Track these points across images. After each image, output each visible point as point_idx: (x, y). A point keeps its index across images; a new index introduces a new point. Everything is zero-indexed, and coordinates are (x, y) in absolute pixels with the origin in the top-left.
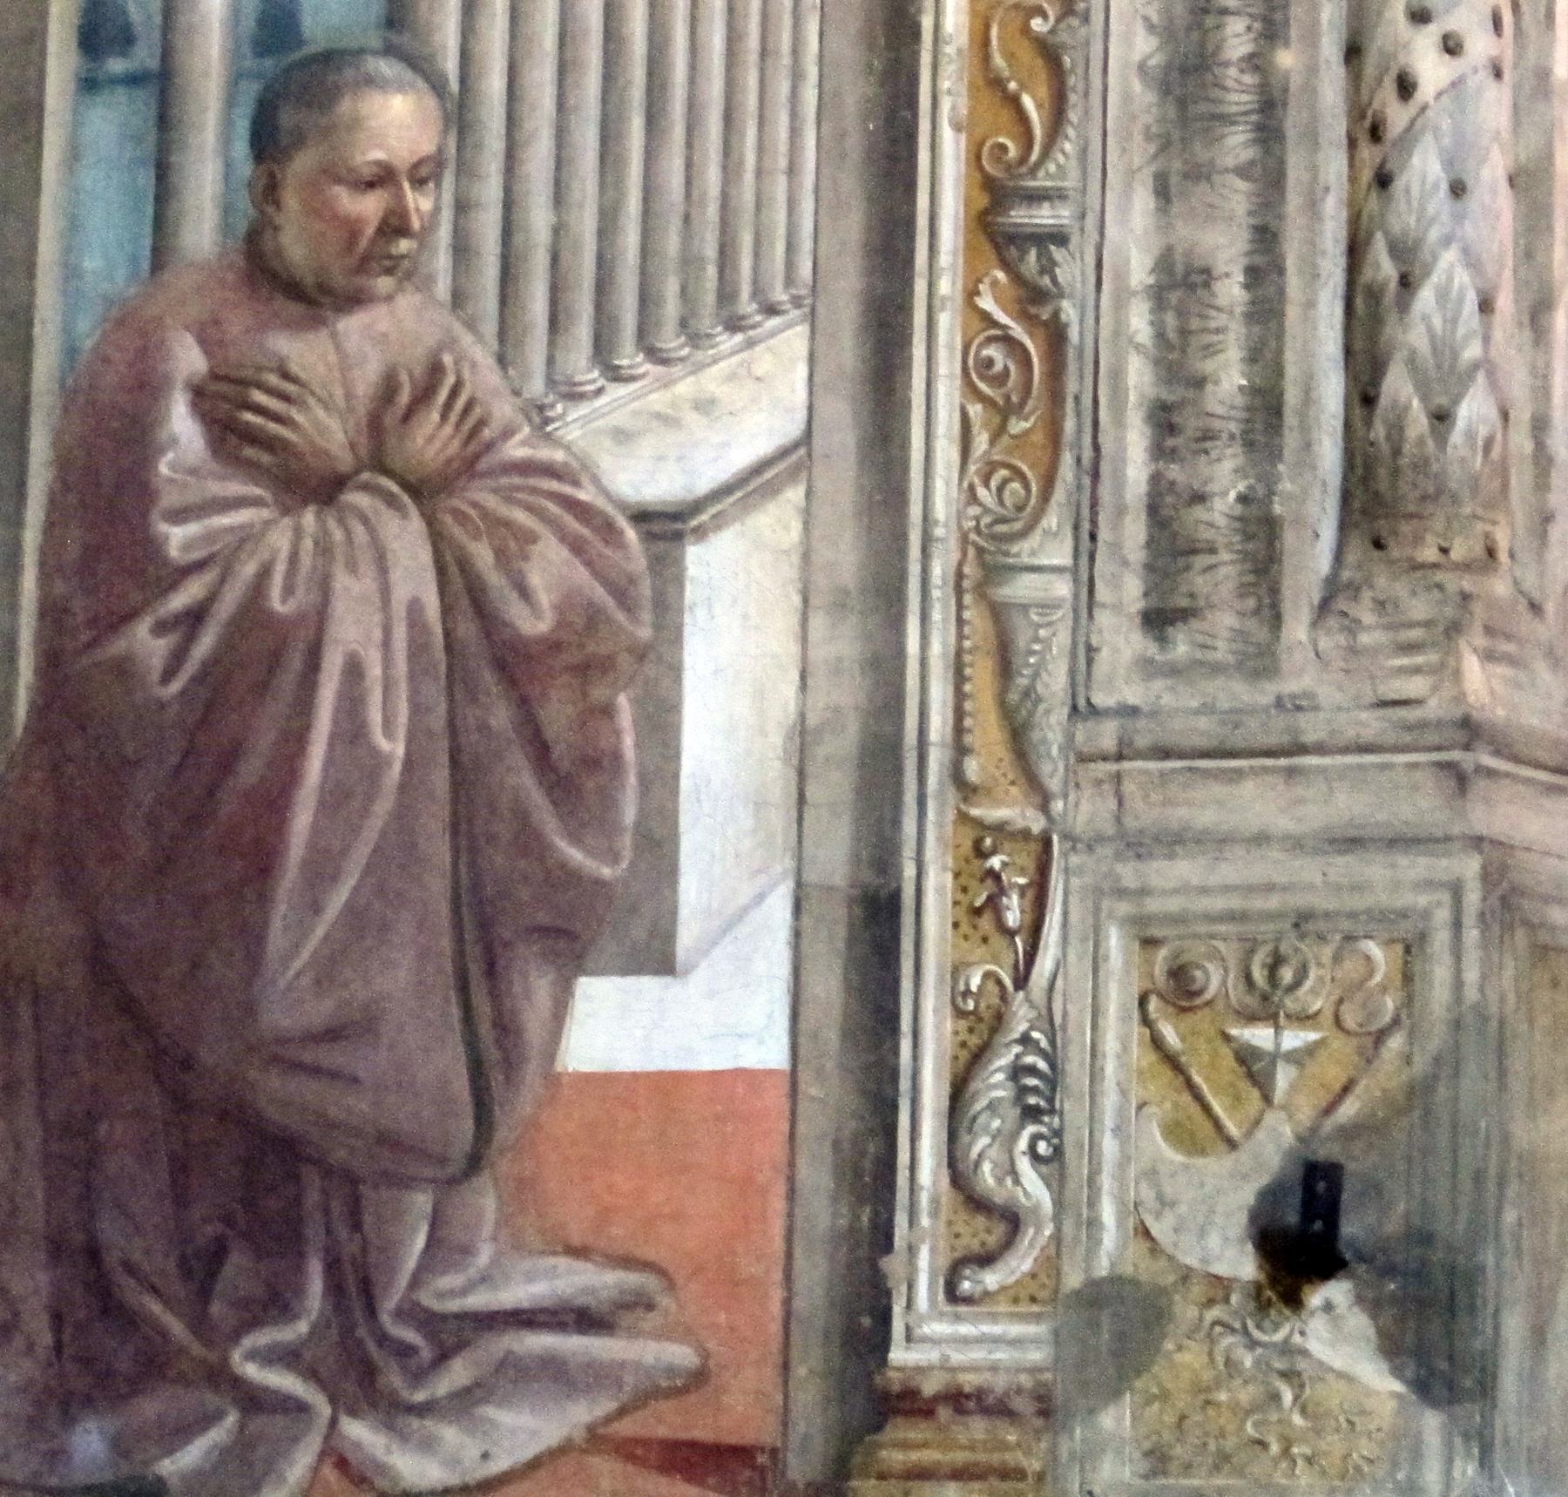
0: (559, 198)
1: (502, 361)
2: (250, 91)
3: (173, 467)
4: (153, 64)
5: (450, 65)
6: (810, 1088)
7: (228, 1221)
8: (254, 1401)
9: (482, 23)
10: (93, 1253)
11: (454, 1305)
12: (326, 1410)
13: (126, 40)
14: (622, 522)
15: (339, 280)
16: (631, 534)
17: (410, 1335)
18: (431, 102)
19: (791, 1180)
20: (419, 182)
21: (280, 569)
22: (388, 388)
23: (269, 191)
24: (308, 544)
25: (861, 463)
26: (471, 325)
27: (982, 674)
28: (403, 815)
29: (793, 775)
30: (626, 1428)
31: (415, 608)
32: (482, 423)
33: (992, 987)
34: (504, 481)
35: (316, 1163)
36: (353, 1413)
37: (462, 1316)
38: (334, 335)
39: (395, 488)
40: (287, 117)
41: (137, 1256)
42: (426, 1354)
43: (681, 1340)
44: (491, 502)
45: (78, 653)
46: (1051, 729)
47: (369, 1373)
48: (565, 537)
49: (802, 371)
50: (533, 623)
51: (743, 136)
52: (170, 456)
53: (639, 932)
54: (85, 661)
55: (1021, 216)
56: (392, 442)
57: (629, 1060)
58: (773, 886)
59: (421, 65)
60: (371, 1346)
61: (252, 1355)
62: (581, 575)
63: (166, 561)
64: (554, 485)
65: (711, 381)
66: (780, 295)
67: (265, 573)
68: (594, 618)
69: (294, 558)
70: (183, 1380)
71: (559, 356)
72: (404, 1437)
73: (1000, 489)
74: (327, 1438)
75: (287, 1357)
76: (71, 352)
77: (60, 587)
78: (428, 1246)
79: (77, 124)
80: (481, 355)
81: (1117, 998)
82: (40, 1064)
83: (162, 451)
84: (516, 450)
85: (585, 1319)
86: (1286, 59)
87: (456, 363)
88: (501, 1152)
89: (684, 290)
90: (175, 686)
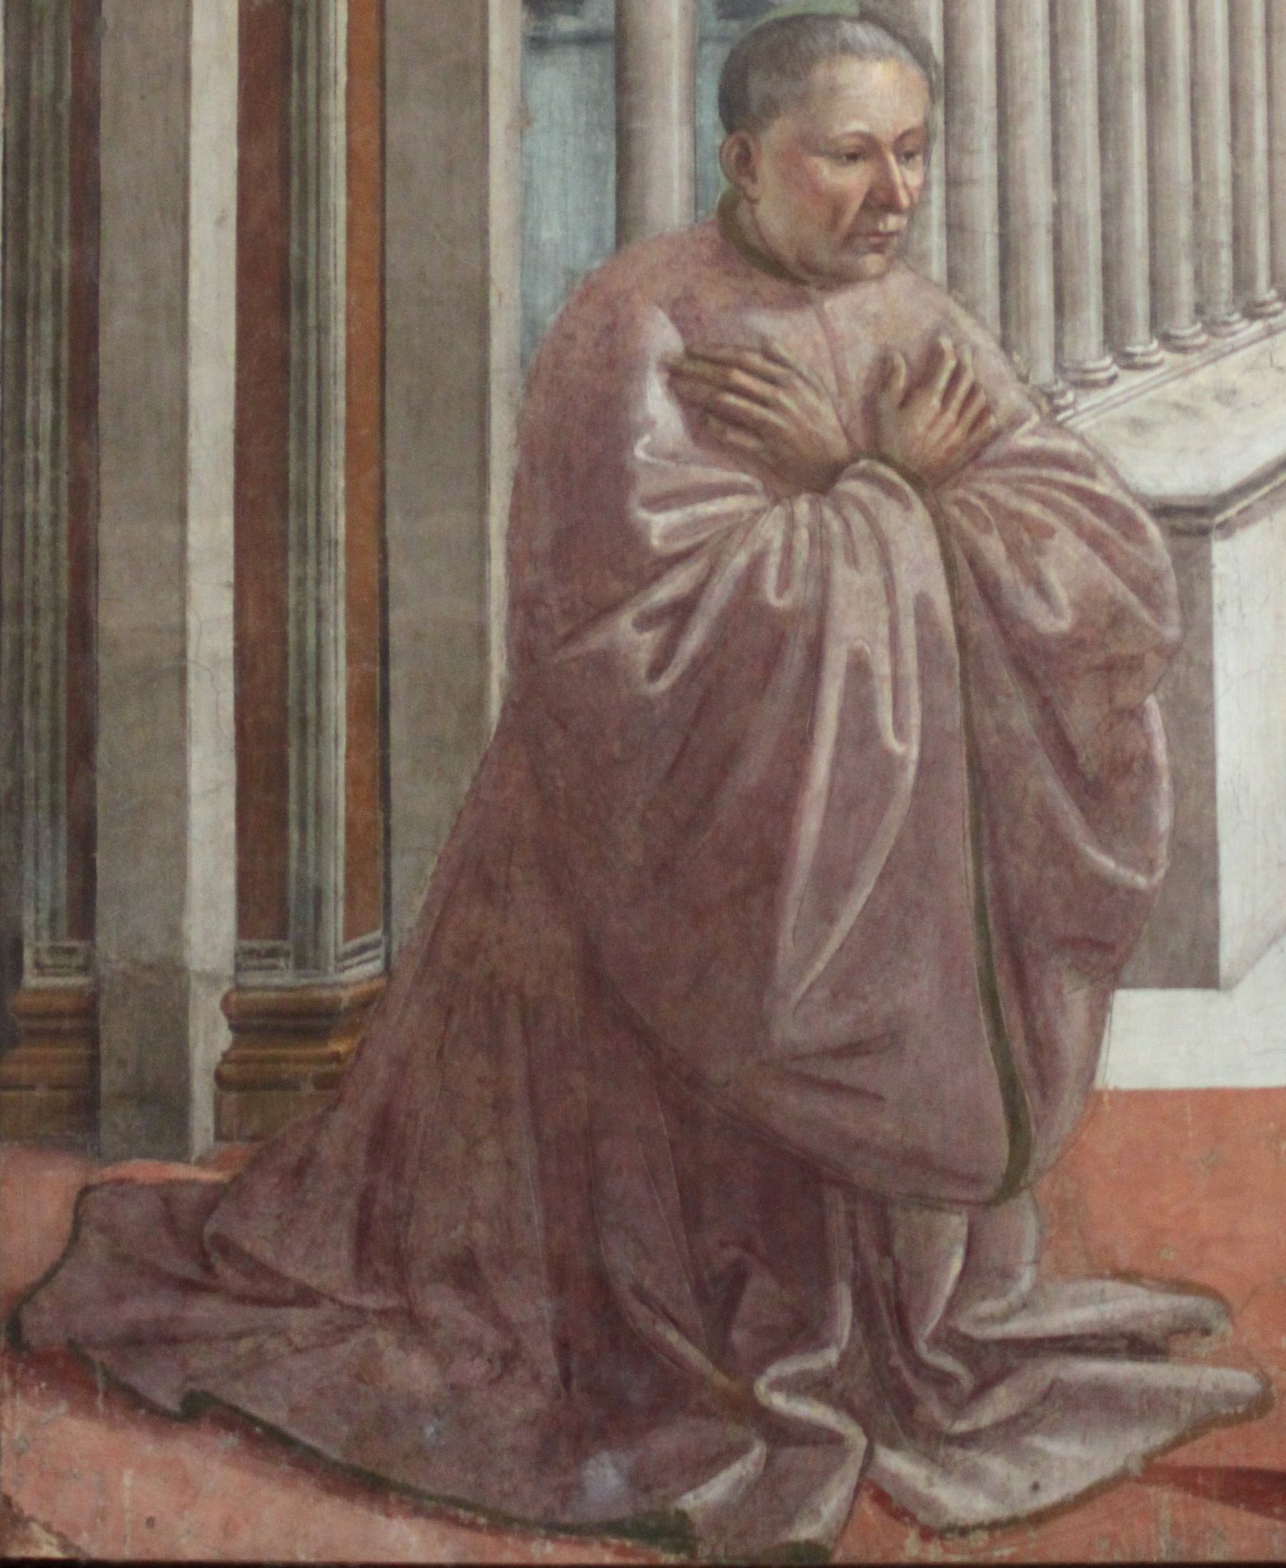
0: (1058, 177)
1: (1006, 345)
2: (716, 55)
3: (651, 451)
4: (608, 23)
5: (934, 35)
7: (747, 1246)
10: (601, 1281)
11: (996, 1331)
12: (862, 1442)
14: (1143, 516)
15: (823, 256)
16: (1153, 530)
17: (948, 1363)
18: (914, 72)
20: (906, 156)
21: (774, 560)
22: (883, 371)
23: (743, 163)
24: (803, 534)
26: (969, 306)
28: (921, 816)
30: (1183, 1457)
31: (923, 605)
32: (985, 412)
35: (836, 1183)
36: (893, 1445)
37: (1006, 1344)
39: (895, 477)
40: (759, 85)
41: (648, 1283)
42: (967, 1380)
43: (1238, 1366)
44: (1000, 493)
47: (906, 1403)
48: (1081, 530)
51: (1250, 114)
52: (646, 439)
54: (562, 655)
57: (1174, 1078)
60: (907, 1375)
61: (778, 1385)
62: (1101, 570)
63: (648, 550)
64: (1067, 477)
65: (1231, 370)
67: (757, 563)
68: (1118, 617)
69: (788, 550)
70: (703, 1411)
71: (1068, 340)
72: (946, 1468)
74: (863, 1471)
75: (818, 1387)
76: (530, 325)
77: (530, 578)
78: (964, 1272)
79: (524, 87)
82: (531, 1079)
83: (638, 435)
84: (1024, 439)
87: (955, 346)
88: (1040, 1173)
89: (1197, 275)
90: (663, 684)
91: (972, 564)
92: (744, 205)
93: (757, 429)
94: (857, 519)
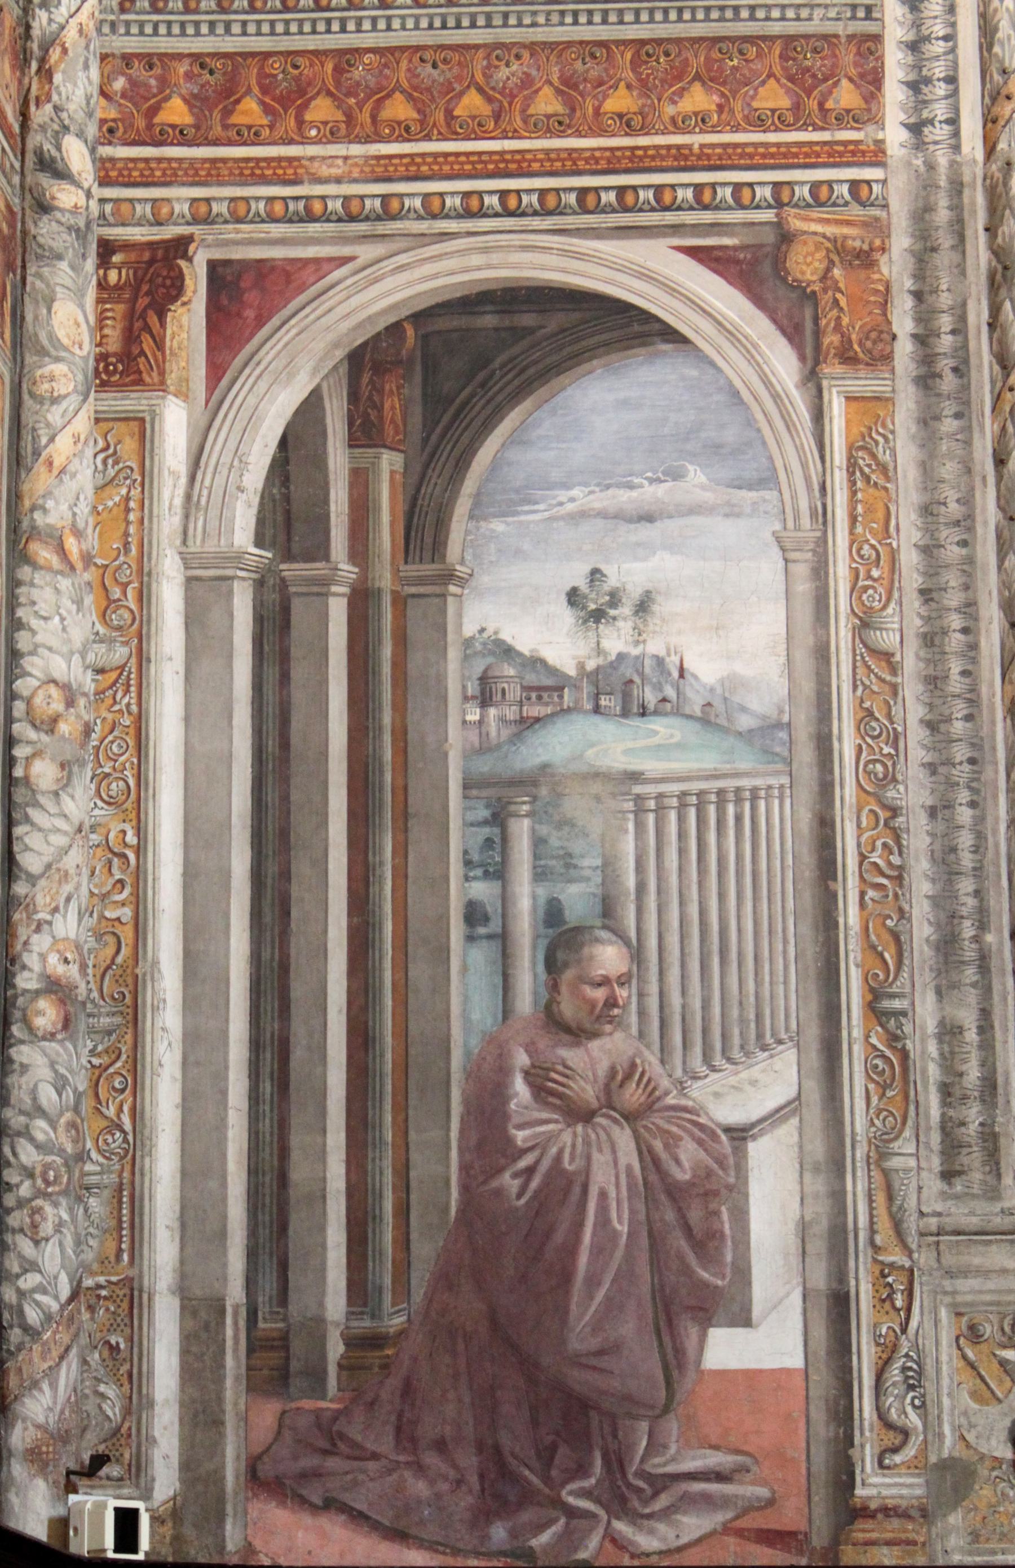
0: (684, 993)
1: (662, 1062)
2: (543, 944)
3: (517, 1106)
4: (499, 930)
5: (633, 934)
6: (814, 1377)
7: (557, 1434)
8: (572, 1512)
9: (646, 916)
10: (497, 1449)
12: (605, 1517)
13: (486, 919)
14: (719, 1132)
15: (587, 1026)
16: (723, 1137)
17: (641, 1484)
18: (624, 950)
19: (807, 1416)
20: (622, 984)
21: (567, 1151)
22: (613, 1072)
23: (554, 987)
24: (580, 1139)
25: (823, 1109)
26: (648, 1046)
27: (880, 1198)
28: (629, 1256)
29: (799, 1241)
31: (629, 1169)
32: (654, 1089)
33: (891, 1333)
34: (667, 1114)
35: (592, 1408)
36: (618, 1518)
38: (587, 1050)
39: (618, 1116)
40: (560, 955)
41: (517, 1449)
42: (649, 1491)
43: (762, 1486)
44: (661, 1123)
45: (478, 1186)
46: (912, 1224)
47: (623, 1500)
48: (694, 1138)
49: (795, 1068)
50: (682, 1175)
53: (736, 1308)
54: (482, 1189)
55: (886, 1004)
56: (615, 1098)
57: (733, 1364)
58: (794, 1289)
60: (624, 1489)
61: (570, 1493)
62: (702, 1154)
63: (516, 1146)
64: (688, 1116)
65: (755, 1072)
66: (783, 1036)
67: (561, 1152)
68: (709, 1174)
69: (574, 1146)
70: (540, 1504)
71: (688, 1059)
72: (640, 1528)
73: (884, 1120)
74: (606, 1530)
75: (586, 1494)
76: (468, 1053)
77: (468, 1157)
79: (465, 955)
80: (652, 1058)
81: (946, 1338)
84: (670, 1100)
85: (720, 1477)
86: (989, 938)
88: (679, 1404)
89: (741, 1033)
90: (522, 1201)
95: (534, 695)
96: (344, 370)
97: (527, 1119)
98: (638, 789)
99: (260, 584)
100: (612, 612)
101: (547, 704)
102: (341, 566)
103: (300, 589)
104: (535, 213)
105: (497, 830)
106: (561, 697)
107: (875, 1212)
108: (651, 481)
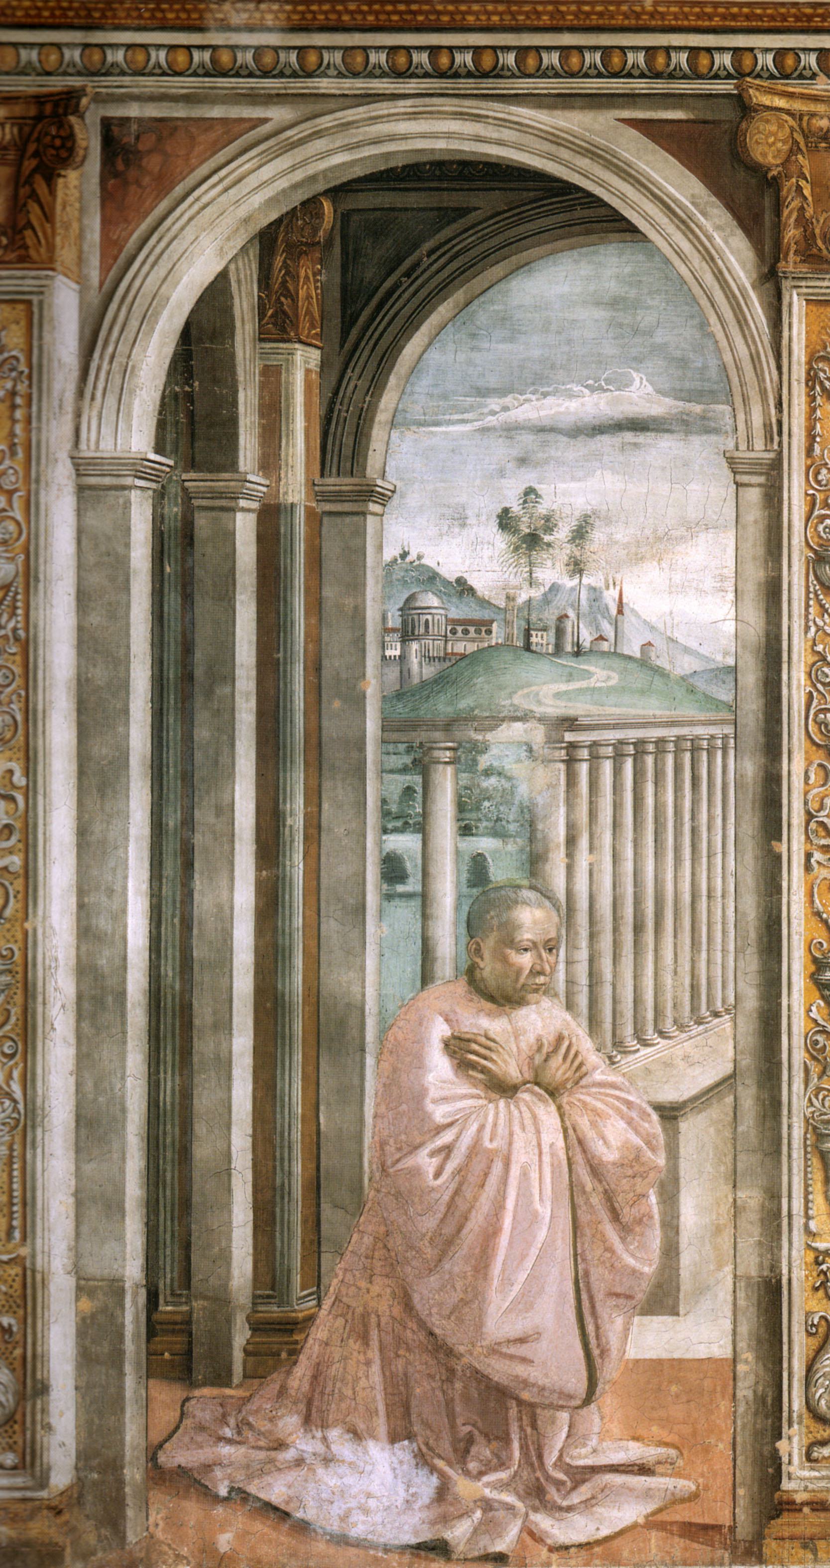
4: (418, 888)
5: (562, 896)
17: (561, 1476)
32: (581, 1065)
33: (823, 1323)
34: (594, 1090)
39: (542, 1092)
59: (547, 895)
64: (617, 1093)
66: (719, 1006)
67: (482, 1128)
73: (823, 1100)
74: (524, 1522)
78: (568, 1437)
83: (431, 1071)
84: (598, 1076)
90: (439, 1181)
91: (575, 1130)
92: (478, 971)
93: (484, 1070)
94: (524, 1109)
95: (460, 629)
96: (254, 252)
97: (446, 1093)
98: (569, 737)
99: (160, 496)
100: (547, 538)
101: (473, 640)
102: (250, 477)
103: (204, 503)
104: (470, 75)
105: (416, 780)
106: (489, 632)
107: (811, 1197)
108: (592, 389)
